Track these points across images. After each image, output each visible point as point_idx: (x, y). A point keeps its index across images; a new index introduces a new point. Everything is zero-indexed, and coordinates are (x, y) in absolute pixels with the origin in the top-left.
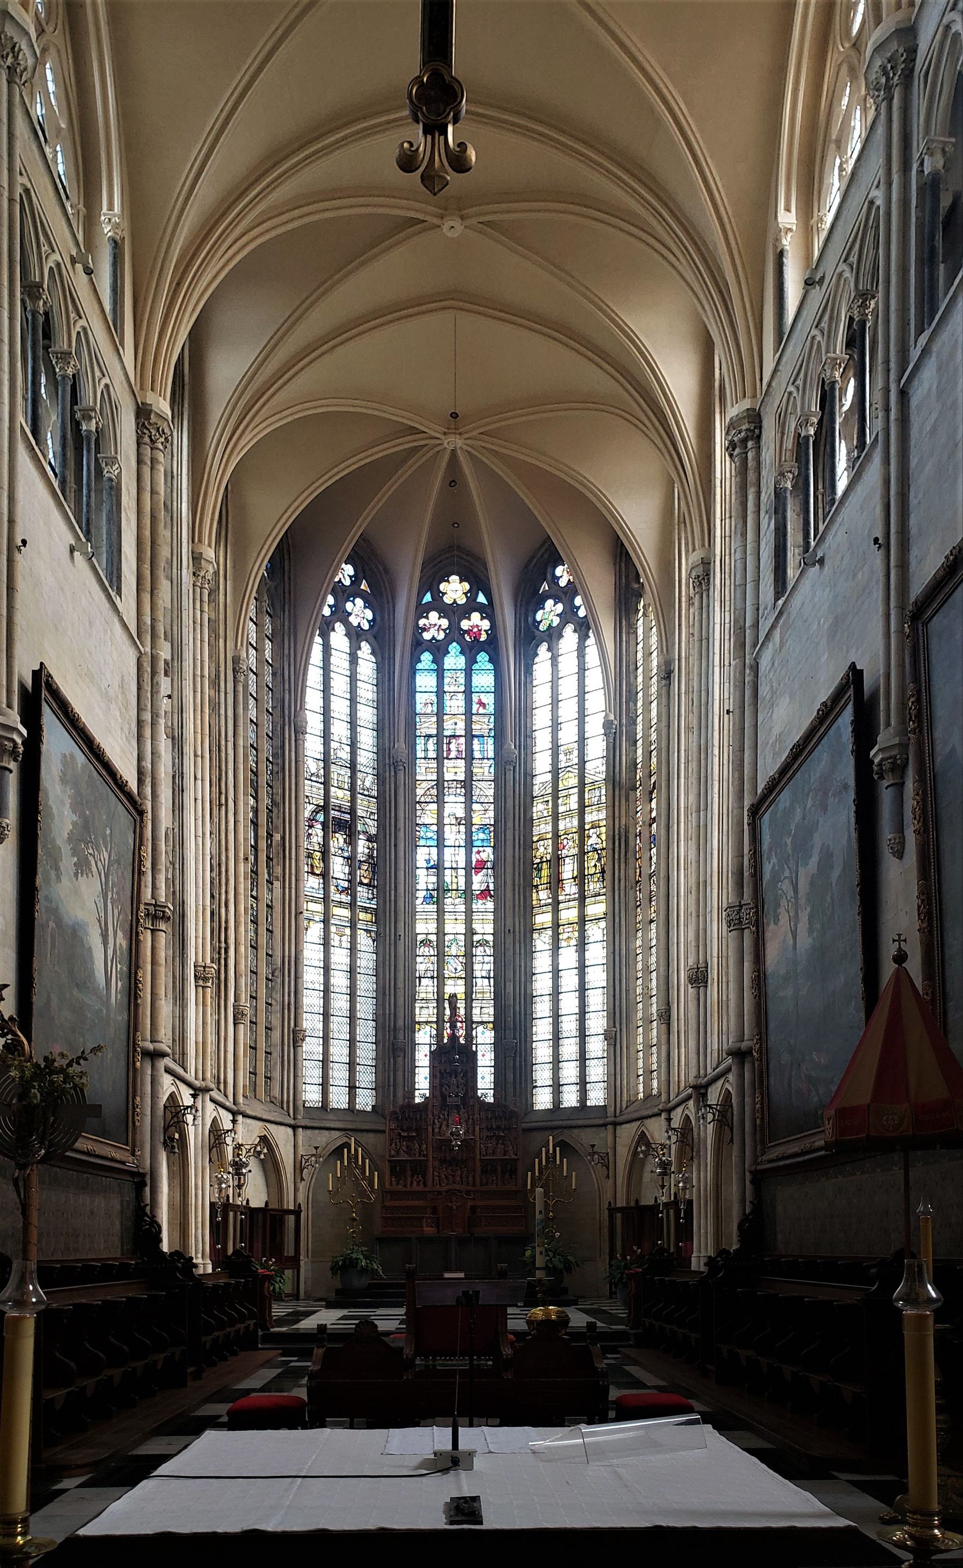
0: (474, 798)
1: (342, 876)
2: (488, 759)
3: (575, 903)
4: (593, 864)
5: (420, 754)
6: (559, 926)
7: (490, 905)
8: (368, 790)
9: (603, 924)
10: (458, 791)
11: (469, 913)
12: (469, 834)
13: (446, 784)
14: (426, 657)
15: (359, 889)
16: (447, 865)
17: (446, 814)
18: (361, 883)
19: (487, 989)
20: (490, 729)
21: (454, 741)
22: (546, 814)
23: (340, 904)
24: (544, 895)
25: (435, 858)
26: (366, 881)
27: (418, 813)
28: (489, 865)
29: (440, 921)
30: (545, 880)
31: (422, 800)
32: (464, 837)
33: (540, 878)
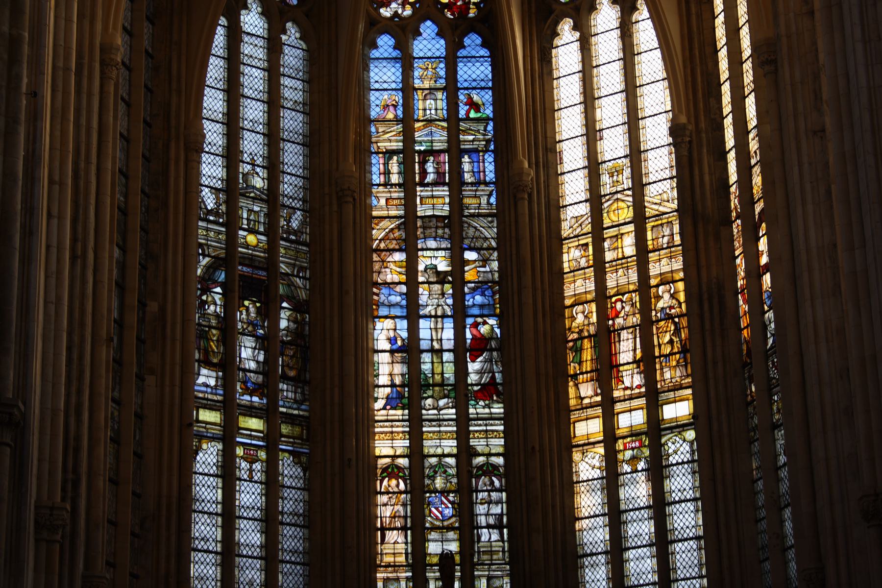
0: (467, 242)
1: (253, 365)
2: (487, 184)
3: (642, 401)
4: (667, 338)
5: (376, 179)
6: (616, 439)
7: (498, 409)
8: (295, 233)
9: (691, 435)
10: (440, 232)
11: (463, 421)
12: (459, 297)
13: (419, 223)
14: (385, 42)
15: (281, 386)
16: (424, 345)
17: (421, 267)
18: (285, 378)
19: (497, 546)
20: (488, 142)
21: (432, 158)
22: (583, 262)
23: (251, 411)
24: (587, 390)
25: (405, 335)
26: (292, 374)
27: (376, 267)
28: (493, 344)
29: (416, 436)
30: (587, 366)
31: (382, 245)
32: (450, 301)
33: (580, 363)
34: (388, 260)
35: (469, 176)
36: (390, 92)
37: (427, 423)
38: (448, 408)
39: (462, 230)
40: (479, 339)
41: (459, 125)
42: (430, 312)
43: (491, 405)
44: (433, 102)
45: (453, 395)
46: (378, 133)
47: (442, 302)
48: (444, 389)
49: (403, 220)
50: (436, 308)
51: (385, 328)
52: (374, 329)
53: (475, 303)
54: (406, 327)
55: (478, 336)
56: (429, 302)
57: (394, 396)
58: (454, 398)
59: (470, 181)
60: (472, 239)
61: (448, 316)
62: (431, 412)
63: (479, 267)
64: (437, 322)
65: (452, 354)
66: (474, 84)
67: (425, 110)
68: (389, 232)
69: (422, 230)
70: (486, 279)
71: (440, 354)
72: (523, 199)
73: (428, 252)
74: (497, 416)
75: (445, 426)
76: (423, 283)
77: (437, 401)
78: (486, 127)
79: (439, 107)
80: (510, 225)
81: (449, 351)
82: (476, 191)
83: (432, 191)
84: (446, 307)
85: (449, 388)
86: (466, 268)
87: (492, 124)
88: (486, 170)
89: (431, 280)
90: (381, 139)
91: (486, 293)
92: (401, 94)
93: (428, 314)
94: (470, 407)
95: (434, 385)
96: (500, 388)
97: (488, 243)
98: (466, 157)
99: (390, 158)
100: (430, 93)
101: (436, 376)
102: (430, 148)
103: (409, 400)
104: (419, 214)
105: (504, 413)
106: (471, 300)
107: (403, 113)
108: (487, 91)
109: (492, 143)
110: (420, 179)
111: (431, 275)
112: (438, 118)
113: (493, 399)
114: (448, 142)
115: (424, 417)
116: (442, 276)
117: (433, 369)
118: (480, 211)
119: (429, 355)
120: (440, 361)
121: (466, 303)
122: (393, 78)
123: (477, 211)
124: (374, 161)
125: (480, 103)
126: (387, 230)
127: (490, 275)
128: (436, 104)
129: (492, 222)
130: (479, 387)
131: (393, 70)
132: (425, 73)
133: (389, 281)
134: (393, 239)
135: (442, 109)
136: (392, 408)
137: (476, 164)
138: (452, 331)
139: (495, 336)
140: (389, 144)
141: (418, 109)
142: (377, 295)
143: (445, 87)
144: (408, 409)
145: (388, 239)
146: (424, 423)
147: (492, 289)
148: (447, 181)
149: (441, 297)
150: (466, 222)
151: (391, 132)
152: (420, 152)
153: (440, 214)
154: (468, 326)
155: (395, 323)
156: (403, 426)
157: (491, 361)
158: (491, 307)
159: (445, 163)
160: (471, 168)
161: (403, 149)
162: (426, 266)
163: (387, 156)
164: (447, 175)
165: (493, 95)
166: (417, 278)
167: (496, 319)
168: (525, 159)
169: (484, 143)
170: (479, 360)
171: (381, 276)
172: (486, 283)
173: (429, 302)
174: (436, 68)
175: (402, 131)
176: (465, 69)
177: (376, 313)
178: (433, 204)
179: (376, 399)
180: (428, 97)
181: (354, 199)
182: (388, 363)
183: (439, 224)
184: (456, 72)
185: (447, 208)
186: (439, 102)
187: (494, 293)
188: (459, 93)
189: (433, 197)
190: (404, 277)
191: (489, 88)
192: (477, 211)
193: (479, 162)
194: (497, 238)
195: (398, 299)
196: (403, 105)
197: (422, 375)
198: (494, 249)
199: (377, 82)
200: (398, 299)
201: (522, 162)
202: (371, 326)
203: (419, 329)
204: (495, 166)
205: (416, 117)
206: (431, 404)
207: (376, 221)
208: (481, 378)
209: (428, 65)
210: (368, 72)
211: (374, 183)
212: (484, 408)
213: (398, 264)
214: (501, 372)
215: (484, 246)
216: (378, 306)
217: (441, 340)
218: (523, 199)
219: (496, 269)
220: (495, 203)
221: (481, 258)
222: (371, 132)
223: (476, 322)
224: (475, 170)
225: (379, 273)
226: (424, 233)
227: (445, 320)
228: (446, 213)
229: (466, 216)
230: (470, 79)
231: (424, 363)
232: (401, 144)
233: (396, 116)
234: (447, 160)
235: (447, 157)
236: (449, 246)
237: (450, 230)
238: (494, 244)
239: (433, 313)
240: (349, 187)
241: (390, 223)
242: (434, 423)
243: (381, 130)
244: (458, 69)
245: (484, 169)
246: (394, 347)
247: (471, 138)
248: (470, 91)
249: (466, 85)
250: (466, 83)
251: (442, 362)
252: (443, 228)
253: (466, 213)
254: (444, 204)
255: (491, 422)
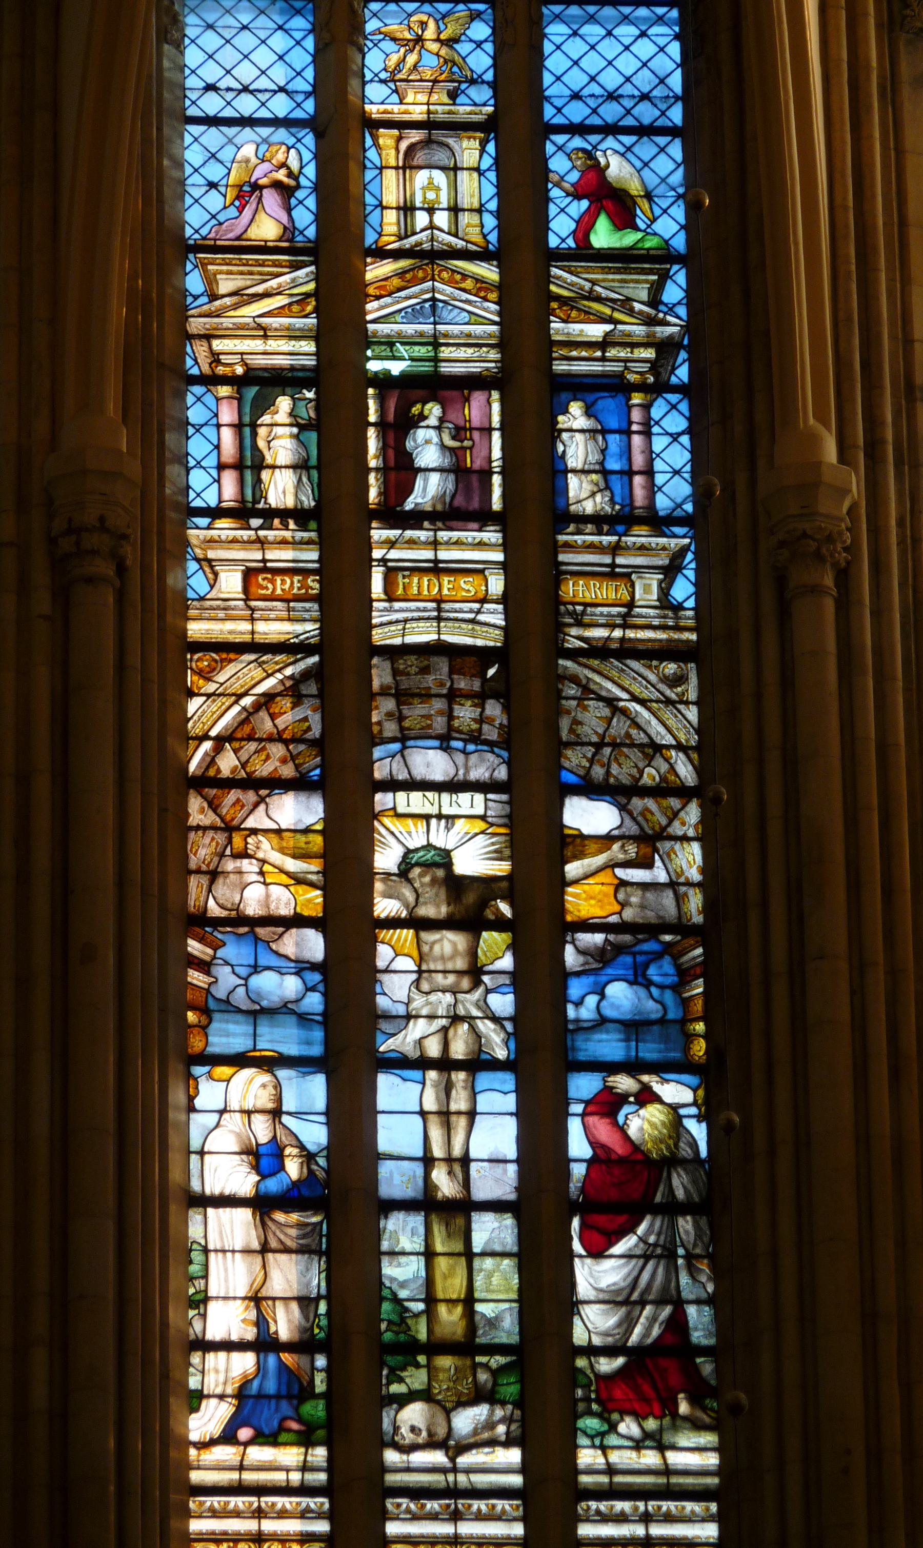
0: (575, 759)
10: (465, 713)
21: (434, 411)
31: (227, 763)
32: (503, 1003)
34: (250, 823)
35: (587, 488)
36: (265, 131)
37: (404, 1502)
38: (493, 1443)
39: (559, 711)
40: (622, 1160)
41: (548, 279)
42: (420, 1042)
43: (667, 1438)
44: (440, 178)
45: (511, 1390)
46: (214, 297)
47: (469, 1003)
48: (475, 1366)
49: (316, 659)
50: (445, 1030)
51: (234, 1105)
52: (191, 1109)
53: (608, 1012)
54: (320, 1103)
55: (619, 1149)
56: (419, 1002)
57: (271, 1387)
58: (518, 1404)
59: (589, 507)
60: (598, 746)
61: (494, 1065)
62: (419, 1458)
63: (627, 864)
64: (448, 1088)
65: (508, 1221)
66: (610, 112)
67: (407, 209)
68: (257, 707)
69: (389, 704)
70: (650, 916)
71: (460, 1221)
72: (816, 590)
73: (416, 796)
74: (690, 1480)
75: (479, 1517)
76: (393, 923)
77: (448, 1413)
78: (656, 290)
79: (468, 199)
80: (759, 697)
81: (496, 1206)
82: (615, 549)
83: (435, 544)
84: (486, 1027)
85: (497, 1361)
86: (573, 869)
87: (681, 277)
88: (658, 465)
89: (428, 911)
90: (226, 322)
91: (653, 972)
92: (309, 140)
93: (414, 1054)
94: (583, 1441)
95: (435, 1347)
96: (706, 1367)
97: (664, 767)
98: (576, 408)
99: (263, 405)
100: (428, 142)
101: (442, 1309)
102: (426, 367)
103: (329, 1408)
104: (379, 637)
105: (720, 1472)
106: (592, 1000)
107: (320, 218)
108: (662, 140)
109: (683, 355)
110: (384, 493)
111: (428, 893)
112: (460, 244)
113: (675, 1414)
114: (502, 345)
115: (392, 1479)
116: (470, 898)
117: (430, 1282)
118: (630, 634)
119: (416, 1221)
120: (459, 1247)
121: (571, 1012)
122: (280, 75)
123: (618, 633)
124: (196, 414)
125: (635, 188)
126: (247, 701)
127: (668, 900)
128: (454, 186)
129: (677, 680)
130: (620, 1361)
131: (279, 42)
132: (411, 59)
133: (252, 909)
134: (270, 739)
135: (480, 211)
136: (264, 1438)
137: (614, 440)
138: (510, 1126)
139: (685, 1151)
140: (257, 345)
141: (383, 207)
142: (205, 967)
143: (492, 118)
144: (328, 1443)
145: (250, 738)
146: (390, 1504)
147: (675, 958)
148: (497, 504)
149: (465, 983)
150: (574, 679)
151: (267, 295)
152: (384, 382)
153: (469, 641)
154: (577, 1108)
155: (278, 1086)
156: (304, 1515)
157: (670, 1255)
158: (674, 1030)
159: (489, 430)
160: (594, 457)
161: (316, 369)
162: (408, 852)
163: (251, 392)
164: (497, 480)
165: (689, 161)
166: (370, 904)
167: (693, 1080)
168: (826, 424)
169: (650, 353)
170: (620, 1248)
171: (222, 889)
172: (652, 930)
173: (419, 1002)
174: (457, 40)
175: (316, 294)
176: (576, 48)
177: (196, 1044)
178: (439, 601)
179: (196, 1399)
180: (420, 157)
181: (121, 570)
182: (247, 1251)
183: (462, 684)
184: (537, 60)
185: (494, 616)
186: (467, 181)
187: (685, 976)
188: (550, 148)
189: (436, 569)
190: (316, 895)
191: (672, 132)
192: (618, 633)
193: (628, 433)
194: (697, 748)
195: (291, 985)
196: (318, 188)
197: (386, 1306)
198: (684, 793)
199: (210, 87)
200: (291, 985)
201: (814, 441)
202: (177, 1096)
203: (374, 1112)
204: (695, 452)
205: (370, 238)
206: (421, 1424)
207: (201, 660)
208: (628, 1323)
209: (423, 25)
210: (179, 47)
211: (198, 503)
212: (638, 1446)
213: (290, 841)
214: (710, 1301)
215: (646, 780)
216: (206, 1012)
217: (465, 1161)
218: (816, 590)
219: (695, 875)
220: (691, 603)
221: (634, 829)
222: (185, 292)
223: (608, 1090)
224: (613, 464)
225: (214, 875)
226: (401, 718)
227: (484, 1079)
228: (489, 639)
229: (573, 654)
230: (594, 89)
231: (392, 1254)
232: (309, 347)
233: (289, 231)
234: (496, 420)
235: (496, 407)
236: (502, 773)
237: (506, 708)
238: (685, 771)
239: (433, 1049)
240: (102, 519)
241: (258, 673)
242: (432, 1505)
243: (225, 285)
244: (548, 47)
245: (650, 462)
246: (273, 1185)
247: (596, 331)
248: (594, 138)
249: (576, 113)
250: (577, 105)
251: (469, 1255)
252: (480, 698)
253: (573, 638)
254: (483, 601)
255: (667, 1506)
